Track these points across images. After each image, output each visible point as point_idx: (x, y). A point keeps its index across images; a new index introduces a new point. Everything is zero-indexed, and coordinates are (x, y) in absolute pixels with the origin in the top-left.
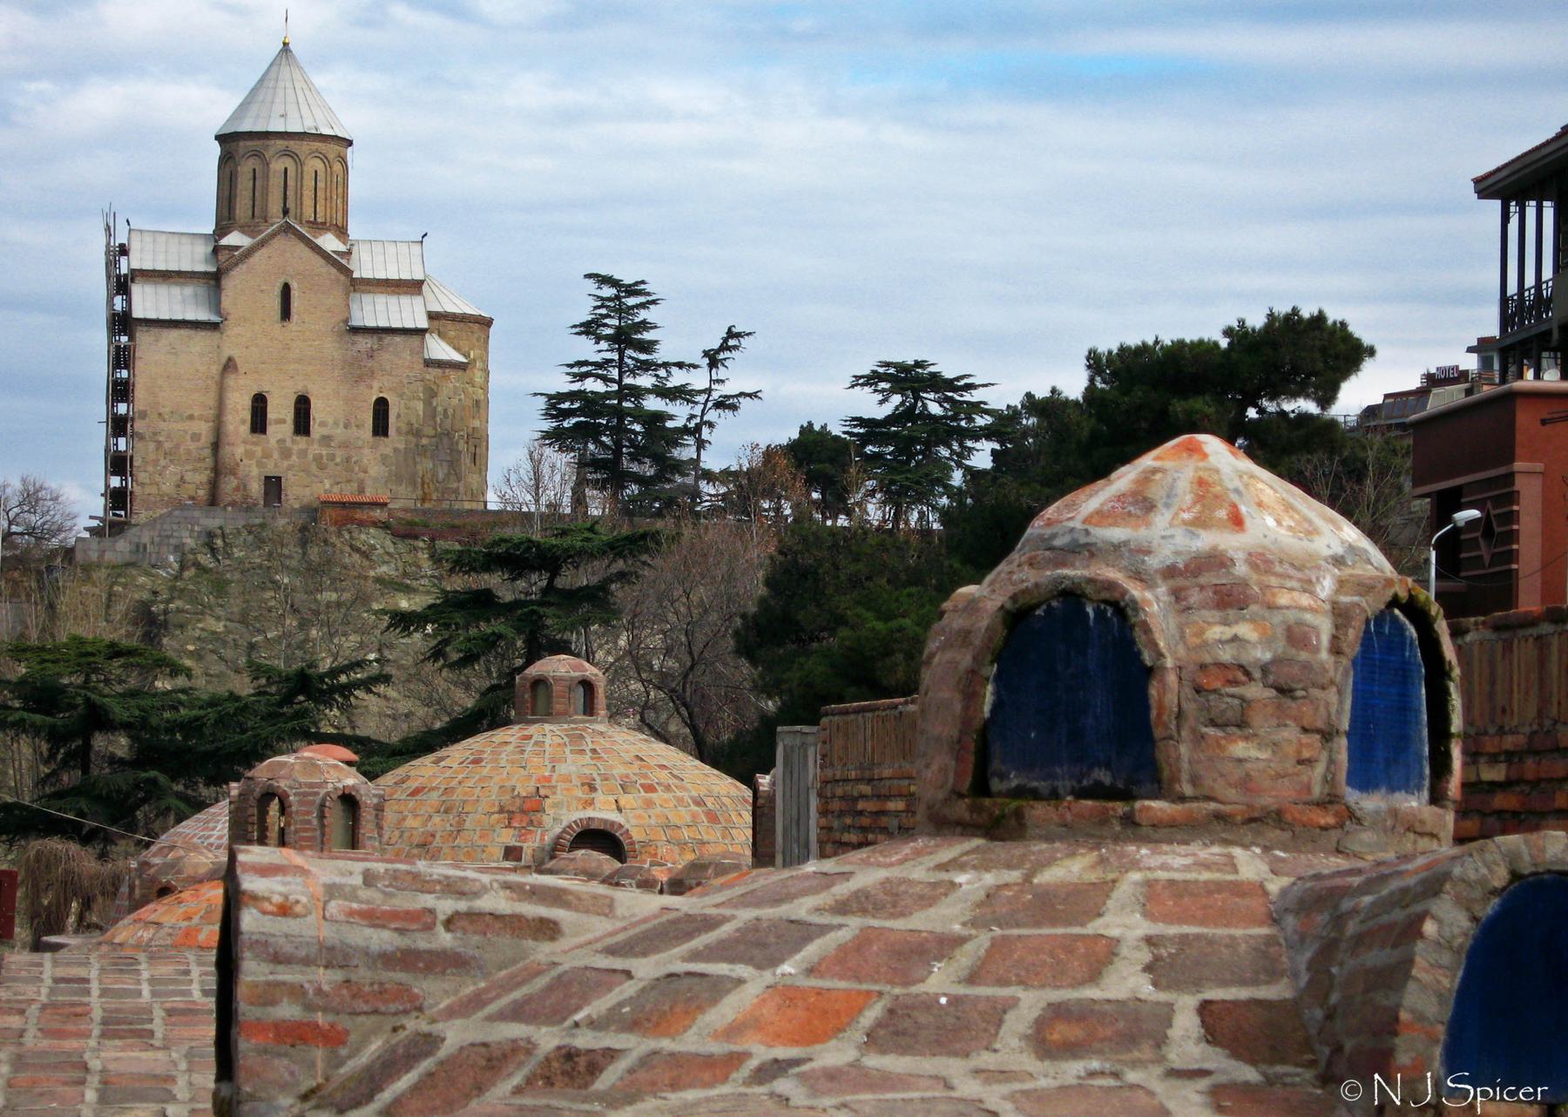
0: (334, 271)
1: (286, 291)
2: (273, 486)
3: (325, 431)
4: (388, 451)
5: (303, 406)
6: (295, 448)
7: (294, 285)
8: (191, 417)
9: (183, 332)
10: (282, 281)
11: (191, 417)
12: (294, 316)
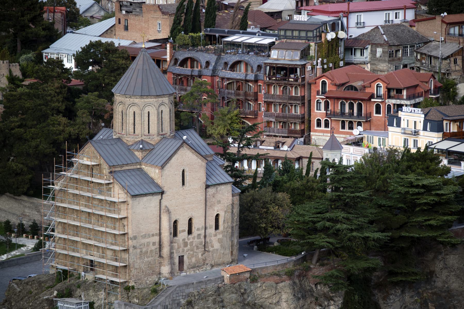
1: (183, 171)
3: (199, 232)
4: (220, 236)
6: (189, 242)
9: (149, 198)
10: (182, 169)
11: (153, 235)
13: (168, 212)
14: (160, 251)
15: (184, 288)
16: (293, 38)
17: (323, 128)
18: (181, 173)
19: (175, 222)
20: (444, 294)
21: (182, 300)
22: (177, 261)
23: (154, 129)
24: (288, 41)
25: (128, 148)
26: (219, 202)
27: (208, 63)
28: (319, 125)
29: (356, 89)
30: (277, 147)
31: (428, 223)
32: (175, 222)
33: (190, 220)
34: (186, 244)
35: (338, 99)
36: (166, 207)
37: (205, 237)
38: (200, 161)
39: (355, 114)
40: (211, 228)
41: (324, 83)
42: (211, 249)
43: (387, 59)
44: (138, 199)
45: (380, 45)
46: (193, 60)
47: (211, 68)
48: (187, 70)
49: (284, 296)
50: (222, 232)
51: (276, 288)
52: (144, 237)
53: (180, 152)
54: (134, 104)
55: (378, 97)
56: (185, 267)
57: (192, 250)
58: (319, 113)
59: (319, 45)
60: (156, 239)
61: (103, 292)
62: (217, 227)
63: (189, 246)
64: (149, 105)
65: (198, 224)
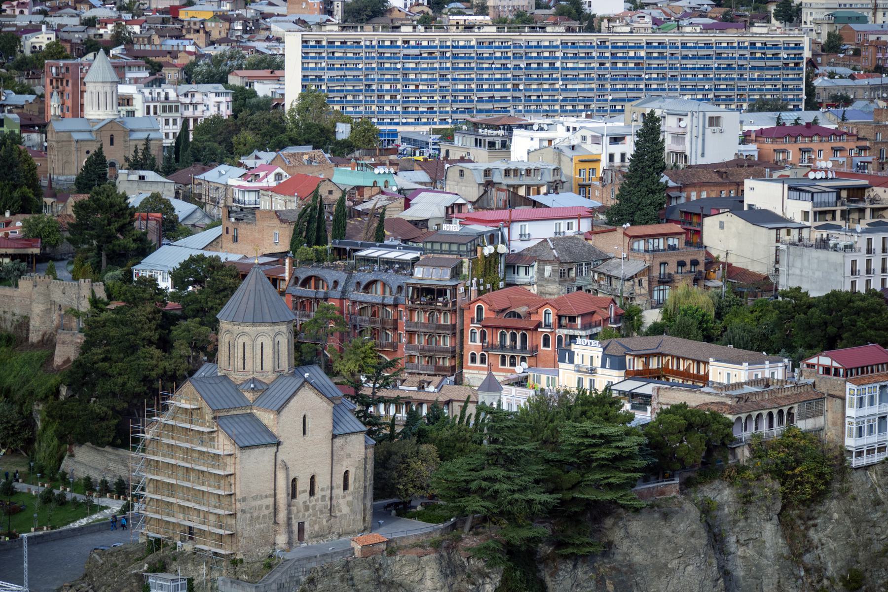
1: (305, 417)
3: (323, 493)
4: (350, 498)
6: (311, 505)
9: (262, 449)
11: (266, 497)
13: (286, 467)
14: (275, 516)
15: (305, 561)
16: (441, 252)
17: (478, 364)
18: (302, 420)
19: (294, 480)
20: (625, 569)
21: (301, 577)
22: (295, 528)
23: (268, 364)
24: (436, 256)
25: (236, 387)
26: (349, 455)
27: (336, 283)
28: (473, 360)
29: (519, 316)
30: (421, 388)
31: (606, 481)
32: (294, 480)
33: (313, 478)
34: (307, 508)
35: (497, 328)
36: (283, 461)
37: (331, 499)
38: (325, 404)
39: (518, 347)
40: (338, 487)
41: (480, 309)
42: (338, 514)
43: (557, 279)
44: (248, 451)
45: (549, 262)
46: (317, 279)
47: (340, 288)
48: (310, 291)
49: (429, 573)
50: (352, 493)
51: (419, 563)
52: (255, 498)
53: (300, 393)
54: (244, 334)
55: (547, 326)
56: (306, 536)
57: (315, 515)
58: (473, 345)
59: (474, 262)
60: (270, 501)
61: (204, 566)
62: (346, 487)
64: (263, 334)
65: (322, 482)
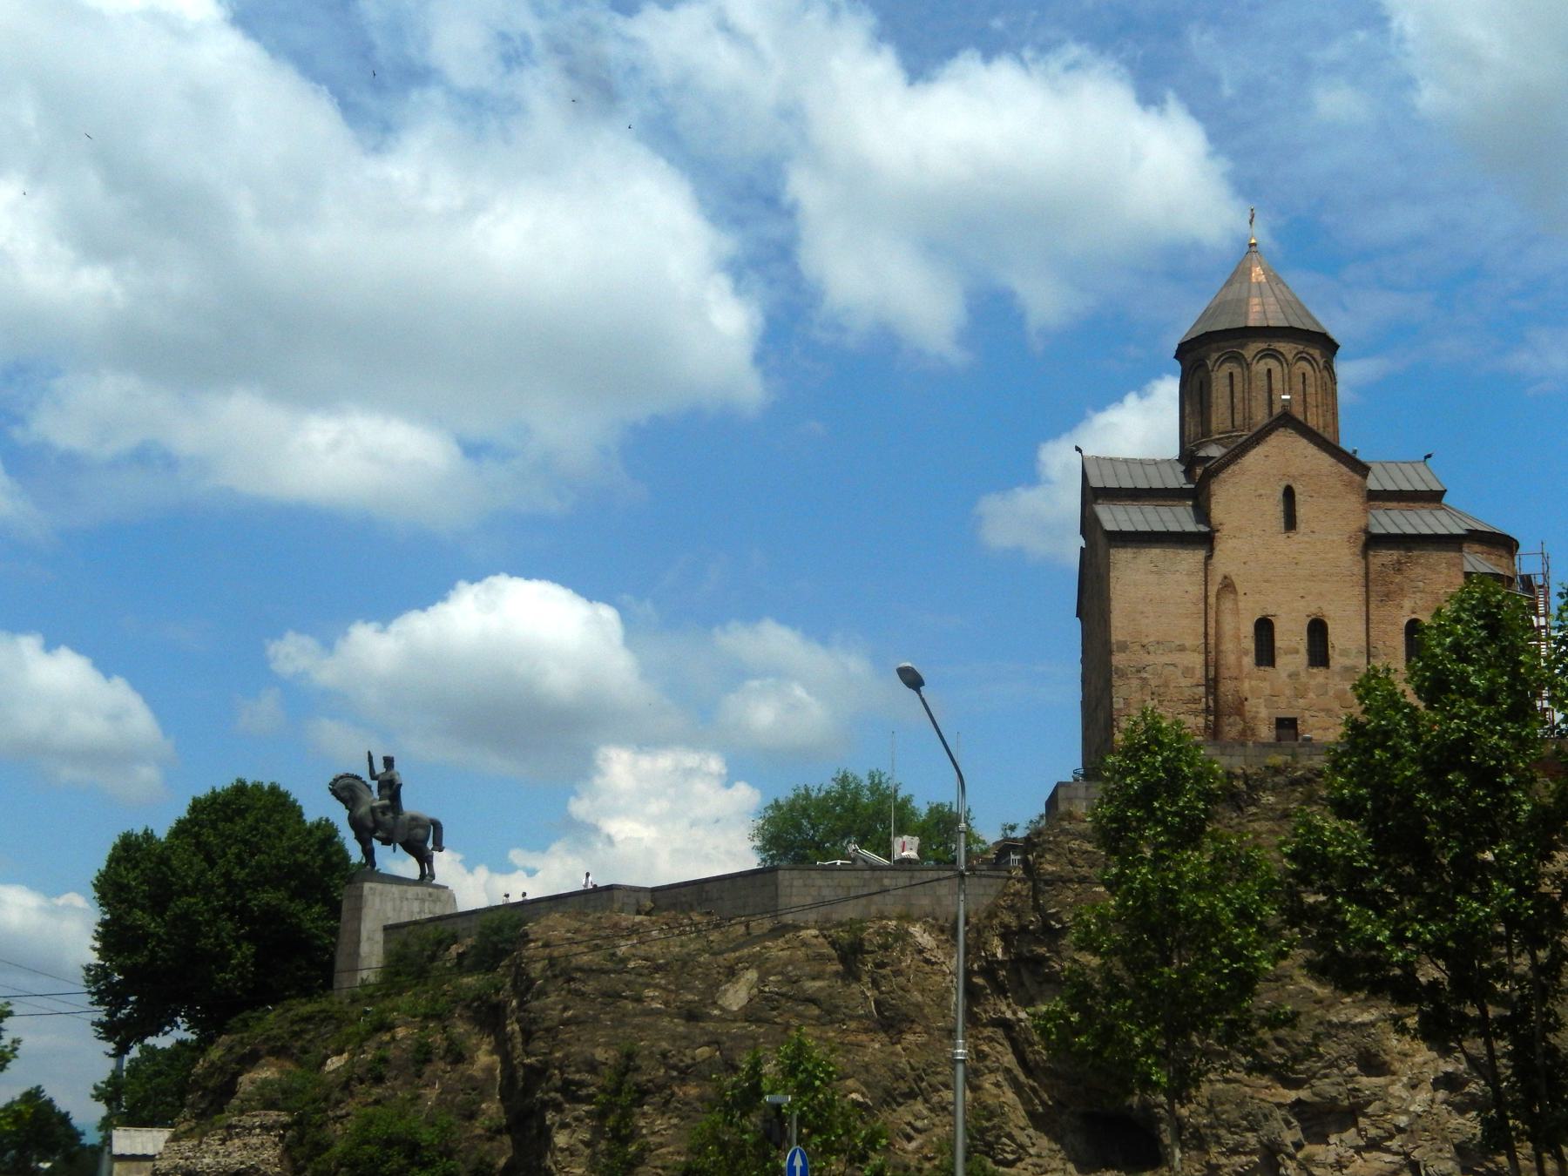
0: (1344, 469)
1: (1289, 494)
2: (1287, 726)
3: (1348, 662)
5: (1318, 630)
7: (1298, 488)
8: (1182, 649)
10: (1284, 484)
11: (1182, 649)
12: (1301, 526)
63: (1311, 695)
65: (1345, 638)
